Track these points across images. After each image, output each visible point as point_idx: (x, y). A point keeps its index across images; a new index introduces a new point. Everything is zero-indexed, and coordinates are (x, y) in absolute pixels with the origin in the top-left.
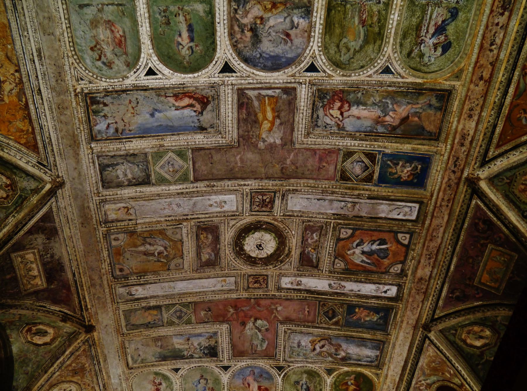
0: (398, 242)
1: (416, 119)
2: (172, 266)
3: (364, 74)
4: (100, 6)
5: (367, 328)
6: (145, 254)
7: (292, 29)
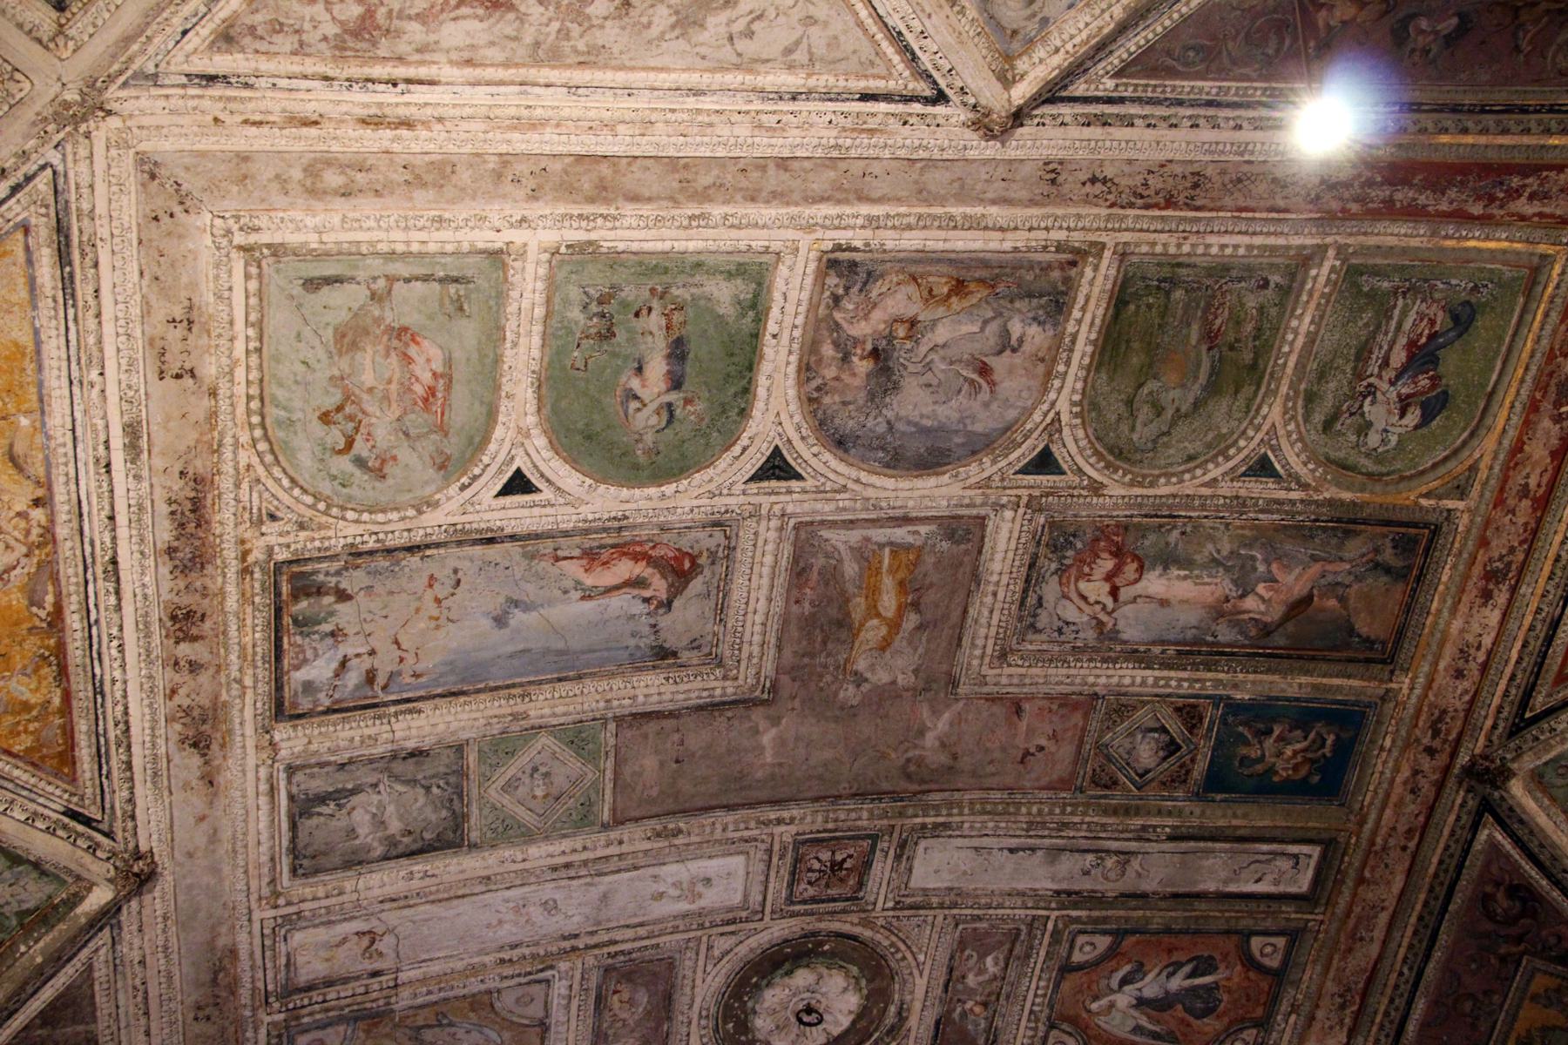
0: (1250, 962)
1: (1332, 603)
3: (1194, 478)
4: (382, 283)
7: (1000, 352)
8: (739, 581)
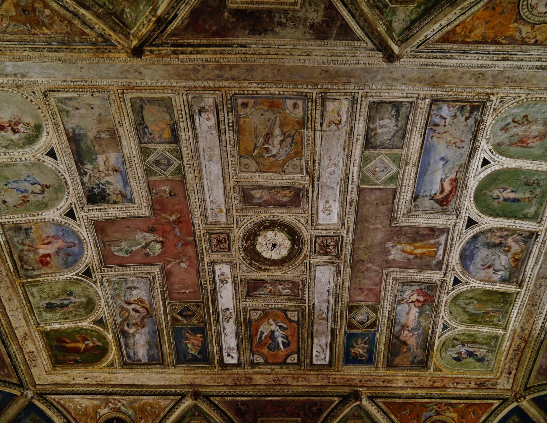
0: (288, 356)
1: (405, 350)
2: (244, 161)
5: (177, 347)
6: (267, 134)
7: (494, 270)
8: (435, 216)
